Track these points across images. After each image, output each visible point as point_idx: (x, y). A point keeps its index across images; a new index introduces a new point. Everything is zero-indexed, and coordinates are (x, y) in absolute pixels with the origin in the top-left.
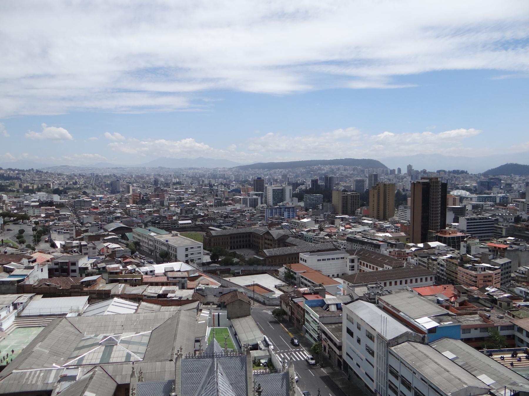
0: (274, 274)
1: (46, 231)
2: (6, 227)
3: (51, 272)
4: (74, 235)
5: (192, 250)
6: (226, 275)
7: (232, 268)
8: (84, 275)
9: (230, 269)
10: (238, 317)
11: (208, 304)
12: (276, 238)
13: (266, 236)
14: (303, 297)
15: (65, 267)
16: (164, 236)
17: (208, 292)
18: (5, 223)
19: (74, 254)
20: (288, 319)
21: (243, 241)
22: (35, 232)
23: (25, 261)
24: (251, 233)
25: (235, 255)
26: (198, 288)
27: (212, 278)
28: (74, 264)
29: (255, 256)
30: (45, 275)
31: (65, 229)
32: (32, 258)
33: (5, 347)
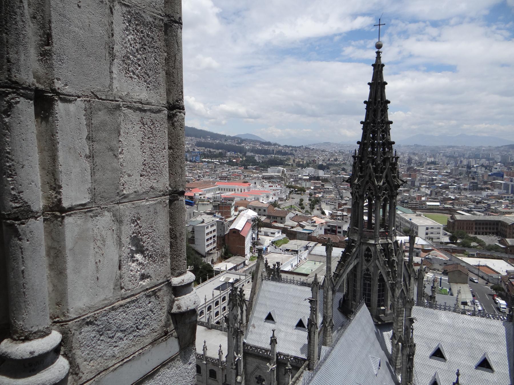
1: (317, 201)
2: (291, 196)
4: (337, 208)
7: (467, 250)
8: (346, 236)
9: (465, 251)
10: (457, 283)
11: (434, 270)
18: (290, 192)
21: (490, 229)
22: (310, 202)
23: (309, 221)
24: (500, 221)
25: (475, 240)
27: (446, 255)
28: (340, 228)
29: (497, 244)
30: (322, 232)
31: (331, 201)
33: (304, 268)
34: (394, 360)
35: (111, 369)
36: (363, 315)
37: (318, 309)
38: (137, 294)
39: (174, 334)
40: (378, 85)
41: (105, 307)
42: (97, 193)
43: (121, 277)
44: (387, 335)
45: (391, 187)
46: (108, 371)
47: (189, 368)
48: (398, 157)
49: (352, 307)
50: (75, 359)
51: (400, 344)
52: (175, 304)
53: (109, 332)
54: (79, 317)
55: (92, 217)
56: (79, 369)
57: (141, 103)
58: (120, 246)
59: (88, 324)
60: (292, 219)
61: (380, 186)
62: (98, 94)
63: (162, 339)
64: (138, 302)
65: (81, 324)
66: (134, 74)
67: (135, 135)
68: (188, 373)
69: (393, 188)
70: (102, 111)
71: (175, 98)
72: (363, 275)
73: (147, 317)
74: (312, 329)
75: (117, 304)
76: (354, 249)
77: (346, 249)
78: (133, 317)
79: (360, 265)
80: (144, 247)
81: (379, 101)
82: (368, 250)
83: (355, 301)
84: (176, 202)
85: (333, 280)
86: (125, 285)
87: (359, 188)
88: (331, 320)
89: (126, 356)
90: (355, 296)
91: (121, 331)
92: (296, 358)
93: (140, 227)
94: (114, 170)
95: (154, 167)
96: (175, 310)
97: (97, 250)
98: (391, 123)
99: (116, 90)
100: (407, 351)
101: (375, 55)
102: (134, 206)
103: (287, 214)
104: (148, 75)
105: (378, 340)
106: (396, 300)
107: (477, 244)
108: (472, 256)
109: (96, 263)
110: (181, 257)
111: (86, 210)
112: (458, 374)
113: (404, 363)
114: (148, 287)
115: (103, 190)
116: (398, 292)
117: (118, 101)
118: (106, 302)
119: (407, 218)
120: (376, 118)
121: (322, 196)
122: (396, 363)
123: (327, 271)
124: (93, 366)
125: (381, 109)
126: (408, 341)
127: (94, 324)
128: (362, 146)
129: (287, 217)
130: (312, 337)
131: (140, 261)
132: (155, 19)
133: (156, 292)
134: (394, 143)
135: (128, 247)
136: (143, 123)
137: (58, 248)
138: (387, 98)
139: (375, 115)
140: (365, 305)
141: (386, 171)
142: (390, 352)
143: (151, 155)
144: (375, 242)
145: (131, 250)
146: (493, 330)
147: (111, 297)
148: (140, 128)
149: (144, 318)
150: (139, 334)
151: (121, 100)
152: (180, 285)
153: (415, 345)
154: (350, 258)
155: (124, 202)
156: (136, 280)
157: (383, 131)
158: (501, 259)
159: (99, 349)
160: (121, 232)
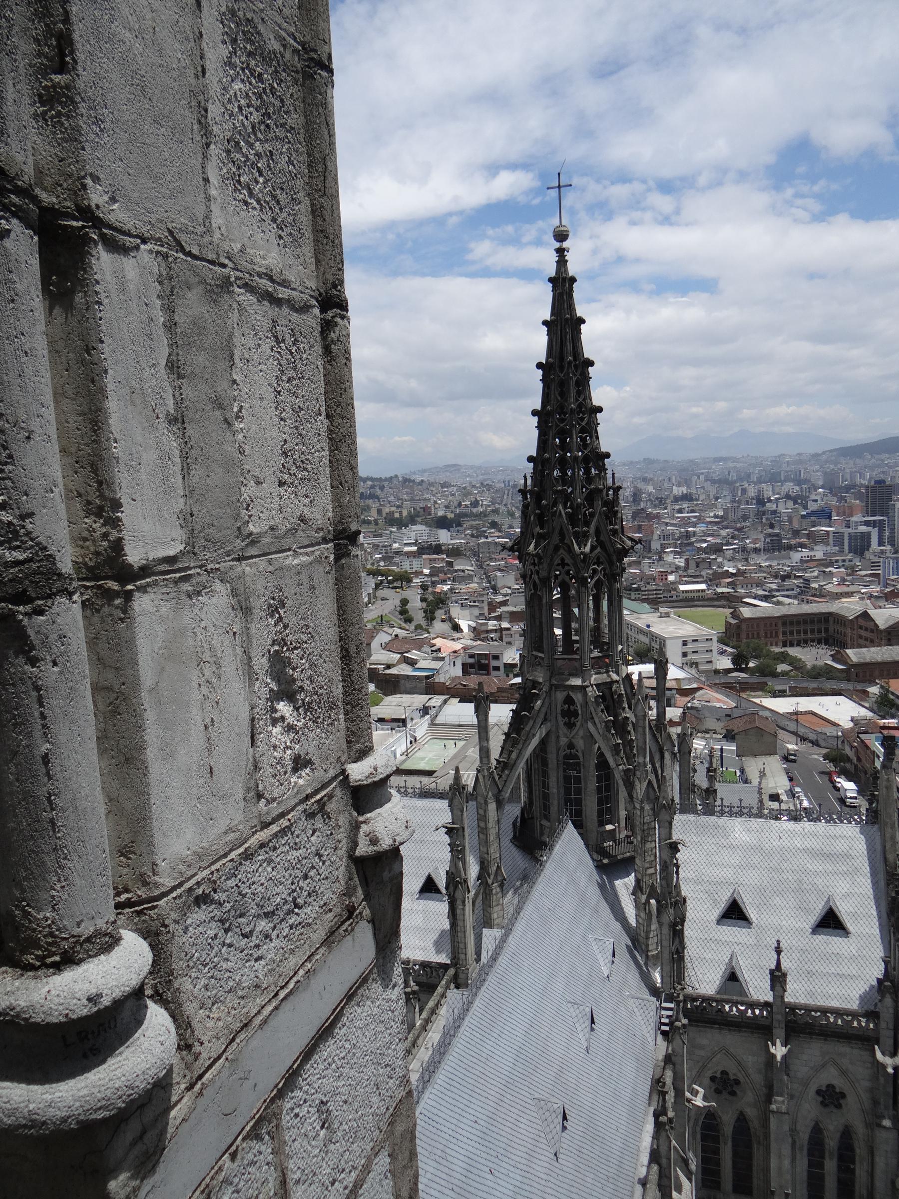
0: (860, 696)
2: (380, 593)
3: (466, 668)
4: (486, 611)
5: (695, 645)
6: (757, 693)
7: (771, 683)
8: (511, 675)
10: (755, 756)
11: (706, 731)
12: (882, 627)
13: (861, 622)
14: (881, 732)
15: (483, 662)
16: (644, 616)
17: (707, 714)
18: (377, 586)
19: (491, 643)
20: (853, 770)
21: (812, 631)
22: (424, 605)
23: (426, 648)
24: (830, 614)
25: (784, 658)
26: (689, 705)
27: (727, 696)
28: (496, 657)
29: (830, 662)
30: (458, 671)
31: (473, 598)
32: (434, 645)
34: (641, 939)
35: (258, 1021)
36: (569, 849)
37: (467, 848)
38: (289, 812)
39: (364, 914)
40: (564, 326)
41: (231, 850)
42: (198, 527)
43: (256, 767)
44: (624, 885)
45: (609, 555)
46: (251, 1030)
47: (394, 997)
48: (619, 488)
49: (542, 834)
50: (180, 1005)
51: (653, 901)
52: (361, 834)
53: (243, 920)
54: (180, 885)
55: (189, 596)
56: (193, 1032)
57: (271, 279)
58: (250, 678)
59: (202, 900)
60: (387, 647)
61: (586, 555)
62: (183, 238)
63: (344, 927)
64: (292, 834)
65: (184, 903)
66: (251, 194)
67: (264, 367)
68: (393, 1012)
69: (614, 558)
70: (194, 291)
71: (331, 278)
72: (561, 758)
73: (312, 873)
74: (458, 895)
75: (253, 842)
76: (539, 703)
77: (519, 703)
78: (287, 875)
79: (553, 738)
80: (294, 680)
81: (570, 363)
82: (569, 700)
83: (547, 818)
84: (343, 561)
85: (497, 777)
86: (265, 787)
87: (540, 563)
88: (499, 868)
89: (281, 983)
90: (546, 808)
91: (266, 915)
92: (424, 965)
93: (286, 627)
94: (229, 464)
95: (303, 462)
96: (364, 848)
97: (205, 690)
98: (600, 410)
99: (217, 235)
100: (670, 915)
101: (554, 257)
102: (271, 568)
103: (373, 637)
104: (278, 202)
105: (606, 899)
106: (638, 806)
107: (790, 668)
108: (781, 694)
109: (206, 727)
110: (362, 708)
111: (178, 575)
112: (778, 951)
113: (665, 943)
114: (309, 791)
115: (209, 519)
116: (640, 788)
117: (224, 266)
118: (231, 837)
119: (641, 624)
120: (566, 400)
121: (451, 590)
122: (647, 945)
123: (481, 758)
124: (219, 1019)
125: (574, 379)
126: (670, 893)
127: (213, 902)
128: (540, 467)
129: (375, 644)
130: (458, 912)
131: (290, 720)
132: (285, 46)
133: (324, 805)
134: (608, 455)
135: (266, 684)
136: (277, 338)
137: (116, 687)
138: (588, 353)
139: (563, 394)
140: (570, 826)
141: (595, 519)
142: (633, 923)
143: (296, 428)
144: (584, 681)
145: (271, 690)
146: (841, 846)
147: (241, 822)
148: (272, 350)
149: (306, 877)
150: (299, 919)
151: (230, 264)
152: (370, 781)
153: (685, 900)
154: (531, 722)
155: (252, 557)
156: (286, 773)
157: (583, 430)
158: (840, 694)
159: (227, 970)
160: (249, 640)
